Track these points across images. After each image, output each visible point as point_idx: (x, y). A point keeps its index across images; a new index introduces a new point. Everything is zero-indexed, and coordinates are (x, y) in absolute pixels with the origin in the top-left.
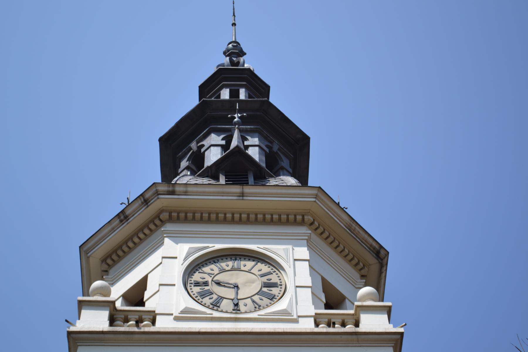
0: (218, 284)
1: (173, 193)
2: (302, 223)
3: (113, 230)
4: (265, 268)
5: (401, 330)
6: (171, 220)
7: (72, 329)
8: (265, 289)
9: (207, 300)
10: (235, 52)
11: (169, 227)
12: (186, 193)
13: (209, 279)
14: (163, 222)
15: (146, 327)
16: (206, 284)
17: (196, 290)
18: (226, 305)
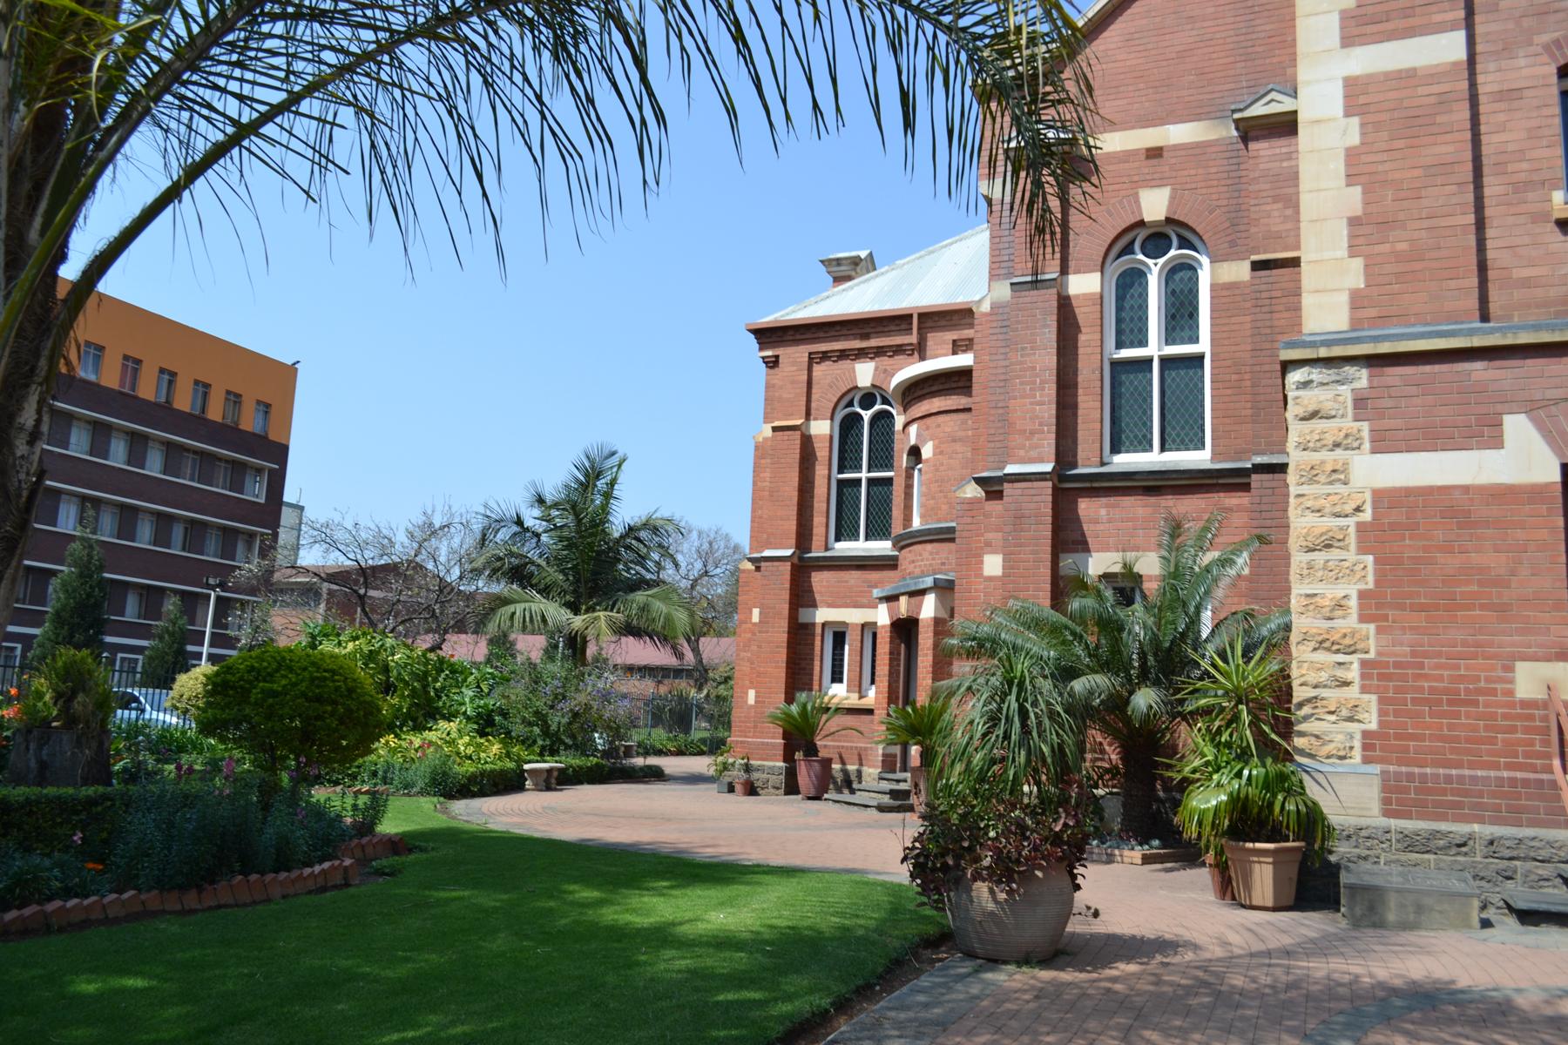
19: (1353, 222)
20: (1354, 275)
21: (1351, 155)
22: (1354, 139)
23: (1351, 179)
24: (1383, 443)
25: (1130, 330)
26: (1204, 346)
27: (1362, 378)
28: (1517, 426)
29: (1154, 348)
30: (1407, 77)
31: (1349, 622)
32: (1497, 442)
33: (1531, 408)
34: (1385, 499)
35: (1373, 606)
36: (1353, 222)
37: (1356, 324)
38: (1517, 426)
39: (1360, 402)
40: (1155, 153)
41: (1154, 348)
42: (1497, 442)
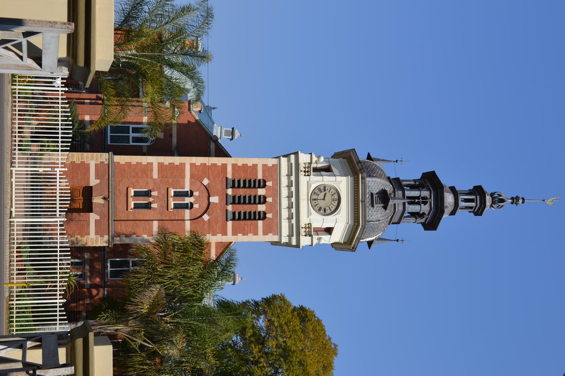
0: (325, 194)
1: (362, 179)
2: (355, 222)
3: (356, 159)
4: (333, 209)
5: (301, 247)
6: (355, 178)
7: (299, 152)
8: (323, 209)
9: (317, 191)
10: (498, 200)
11: (353, 178)
12: (362, 183)
13: (327, 191)
14: (354, 176)
15: (302, 174)
16: (325, 190)
17: (322, 188)
18: (315, 197)
19: (130, 163)
20: (122, 162)
21: (141, 163)
22: (143, 163)
23: (137, 163)
24: (96, 165)
25: (135, 130)
26: (131, 144)
27: (107, 162)
28: (98, 181)
29: (132, 135)
30: (152, 171)
31: (71, 160)
32: (96, 179)
33: (100, 183)
34: (88, 165)
35: (73, 163)
36: (130, 163)
37: (115, 162)
38: (98, 181)
39: (102, 162)
40: (171, 136)
41: (132, 135)
42: (96, 179)
